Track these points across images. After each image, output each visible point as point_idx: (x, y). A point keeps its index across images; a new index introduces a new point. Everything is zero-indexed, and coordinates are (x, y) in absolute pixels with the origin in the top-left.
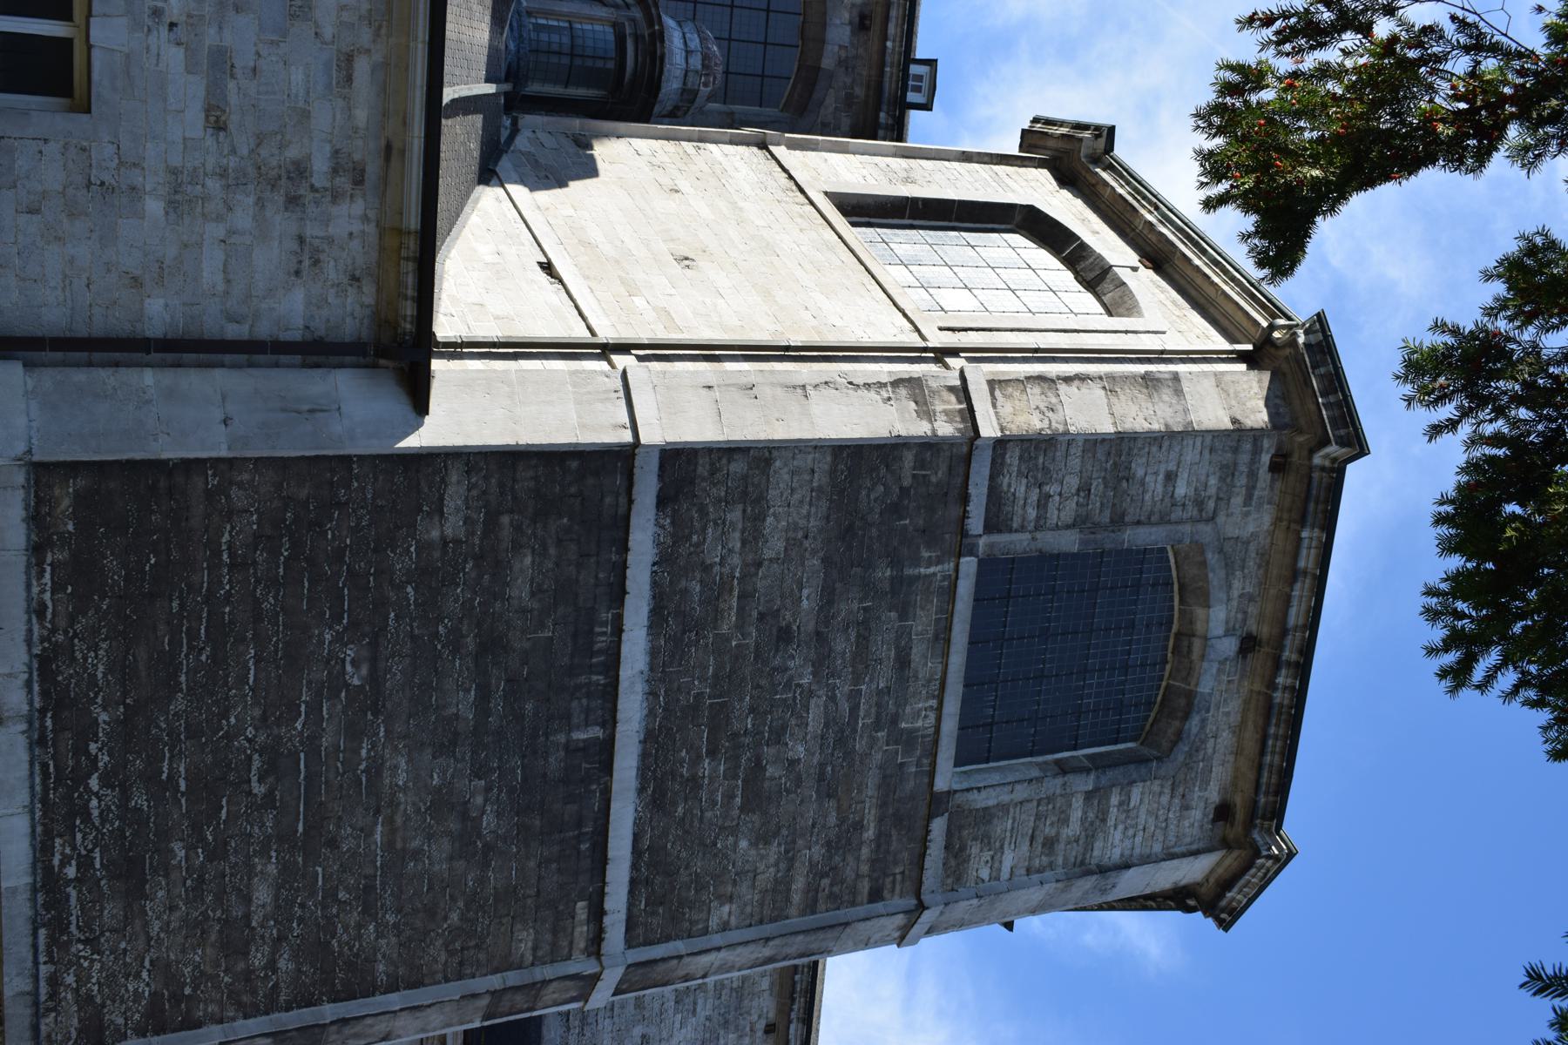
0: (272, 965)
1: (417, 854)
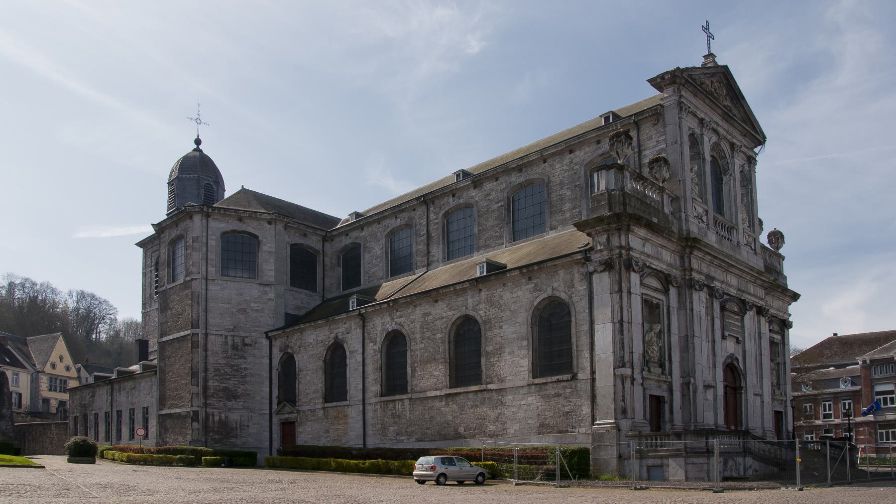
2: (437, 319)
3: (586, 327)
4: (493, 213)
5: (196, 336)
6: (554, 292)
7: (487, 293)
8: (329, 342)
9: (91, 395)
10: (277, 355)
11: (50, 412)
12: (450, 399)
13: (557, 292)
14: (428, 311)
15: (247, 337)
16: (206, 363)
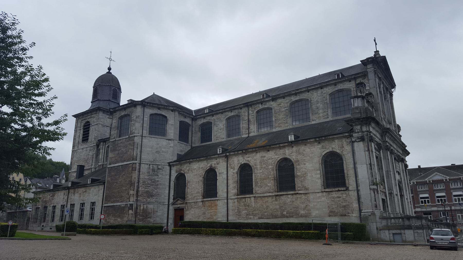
0: (128, 187)
1: (124, 178)
2: (269, 159)
3: (352, 166)
4: (282, 112)
5: (135, 164)
6: (333, 149)
7: (296, 148)
8: (206, 168)
9: (52, 195)
10: (174, 174)
12: (278, 197)
13: (335, 150)
14: (264, 155)
15: (159, 165)
16: (139, 178)
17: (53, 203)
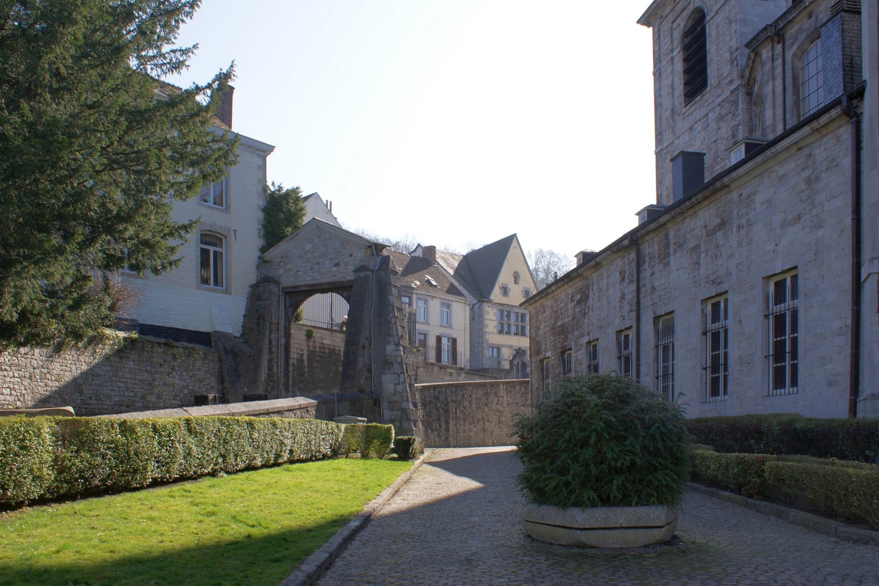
9: (578, 297)
11: (501, 368)
17: (586, 330)
